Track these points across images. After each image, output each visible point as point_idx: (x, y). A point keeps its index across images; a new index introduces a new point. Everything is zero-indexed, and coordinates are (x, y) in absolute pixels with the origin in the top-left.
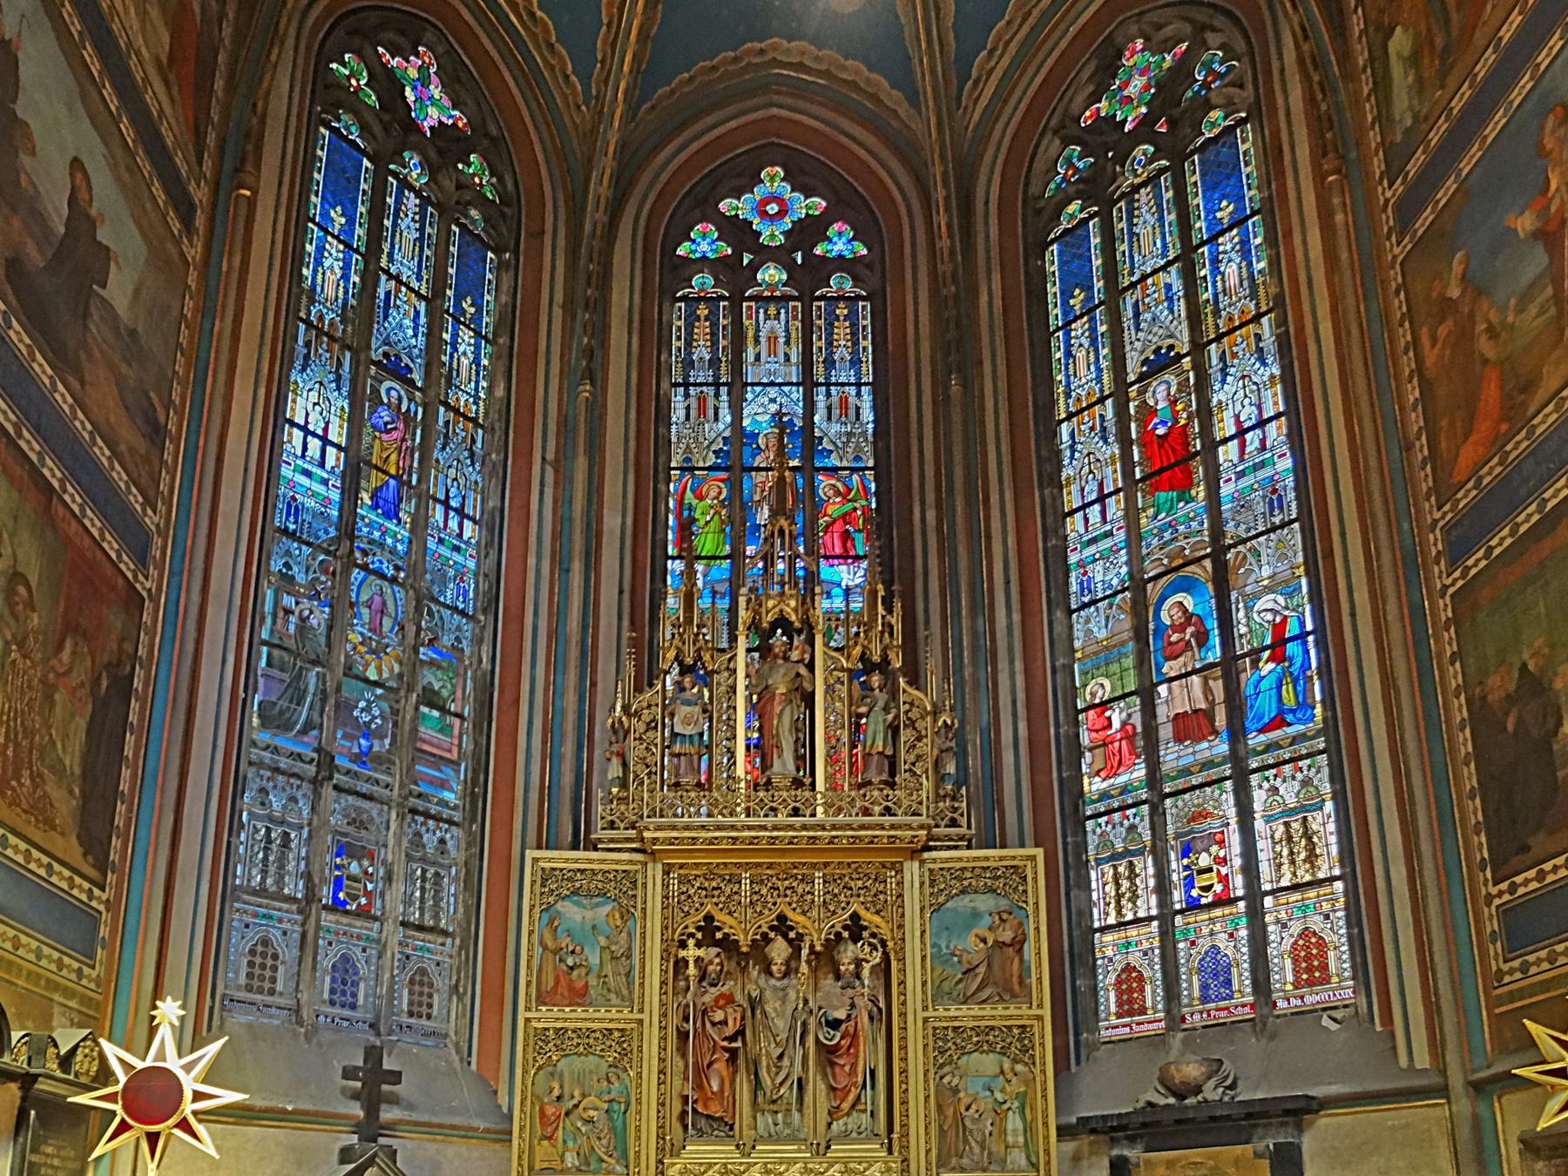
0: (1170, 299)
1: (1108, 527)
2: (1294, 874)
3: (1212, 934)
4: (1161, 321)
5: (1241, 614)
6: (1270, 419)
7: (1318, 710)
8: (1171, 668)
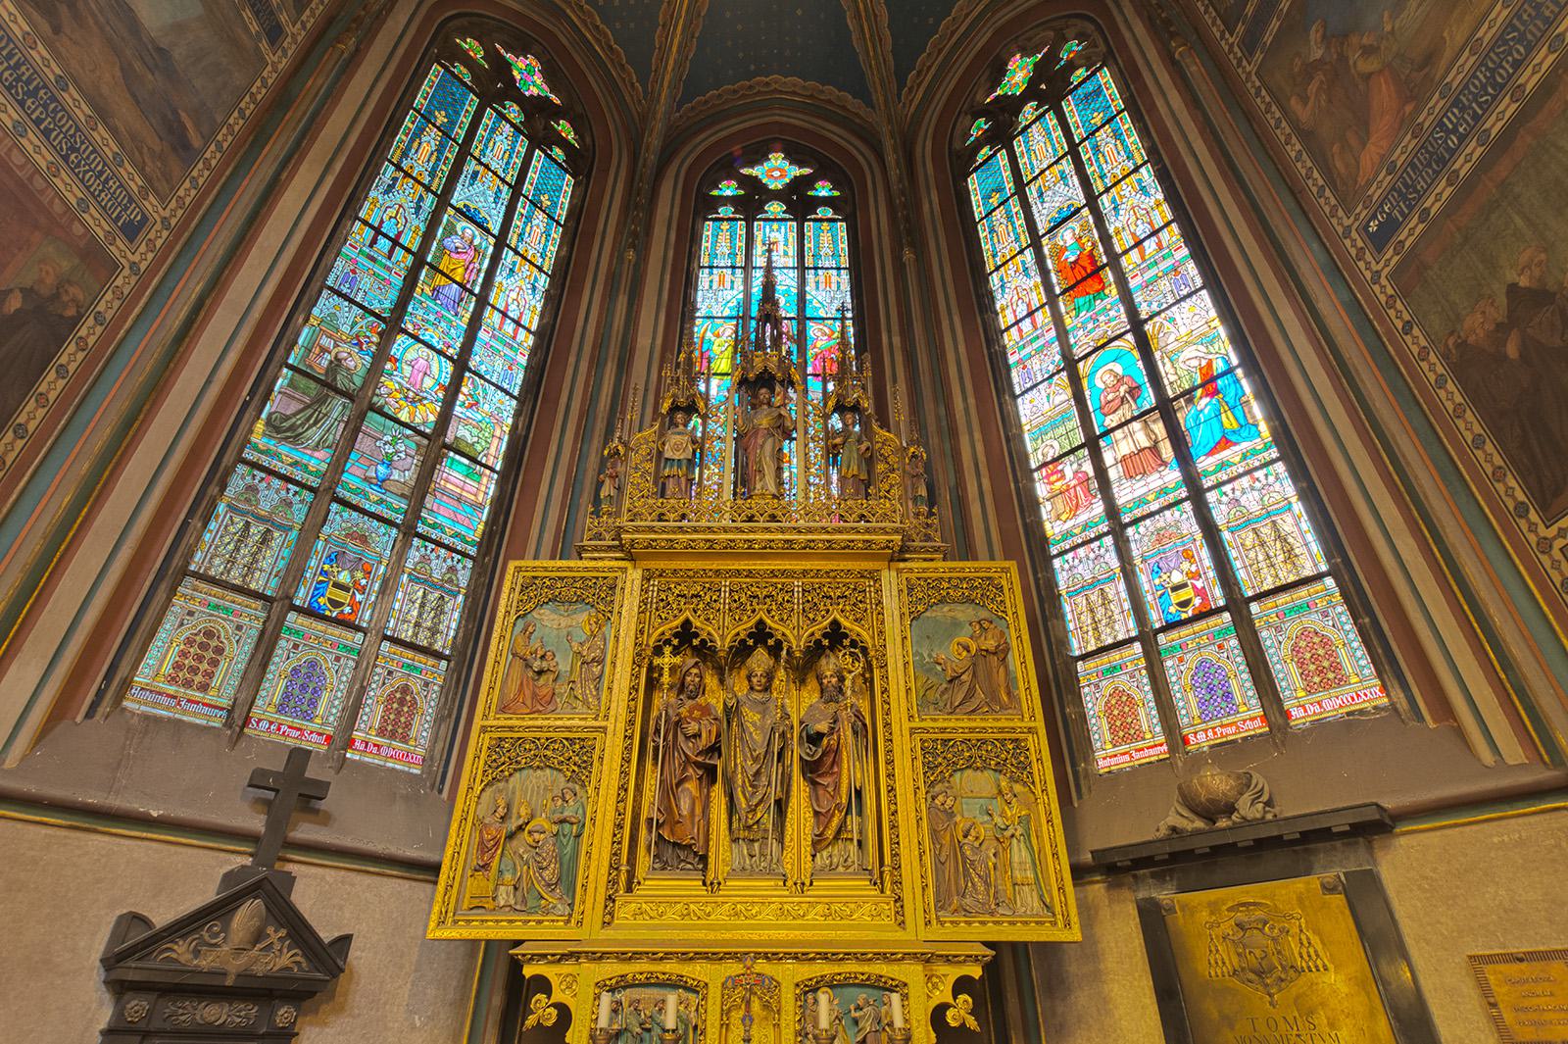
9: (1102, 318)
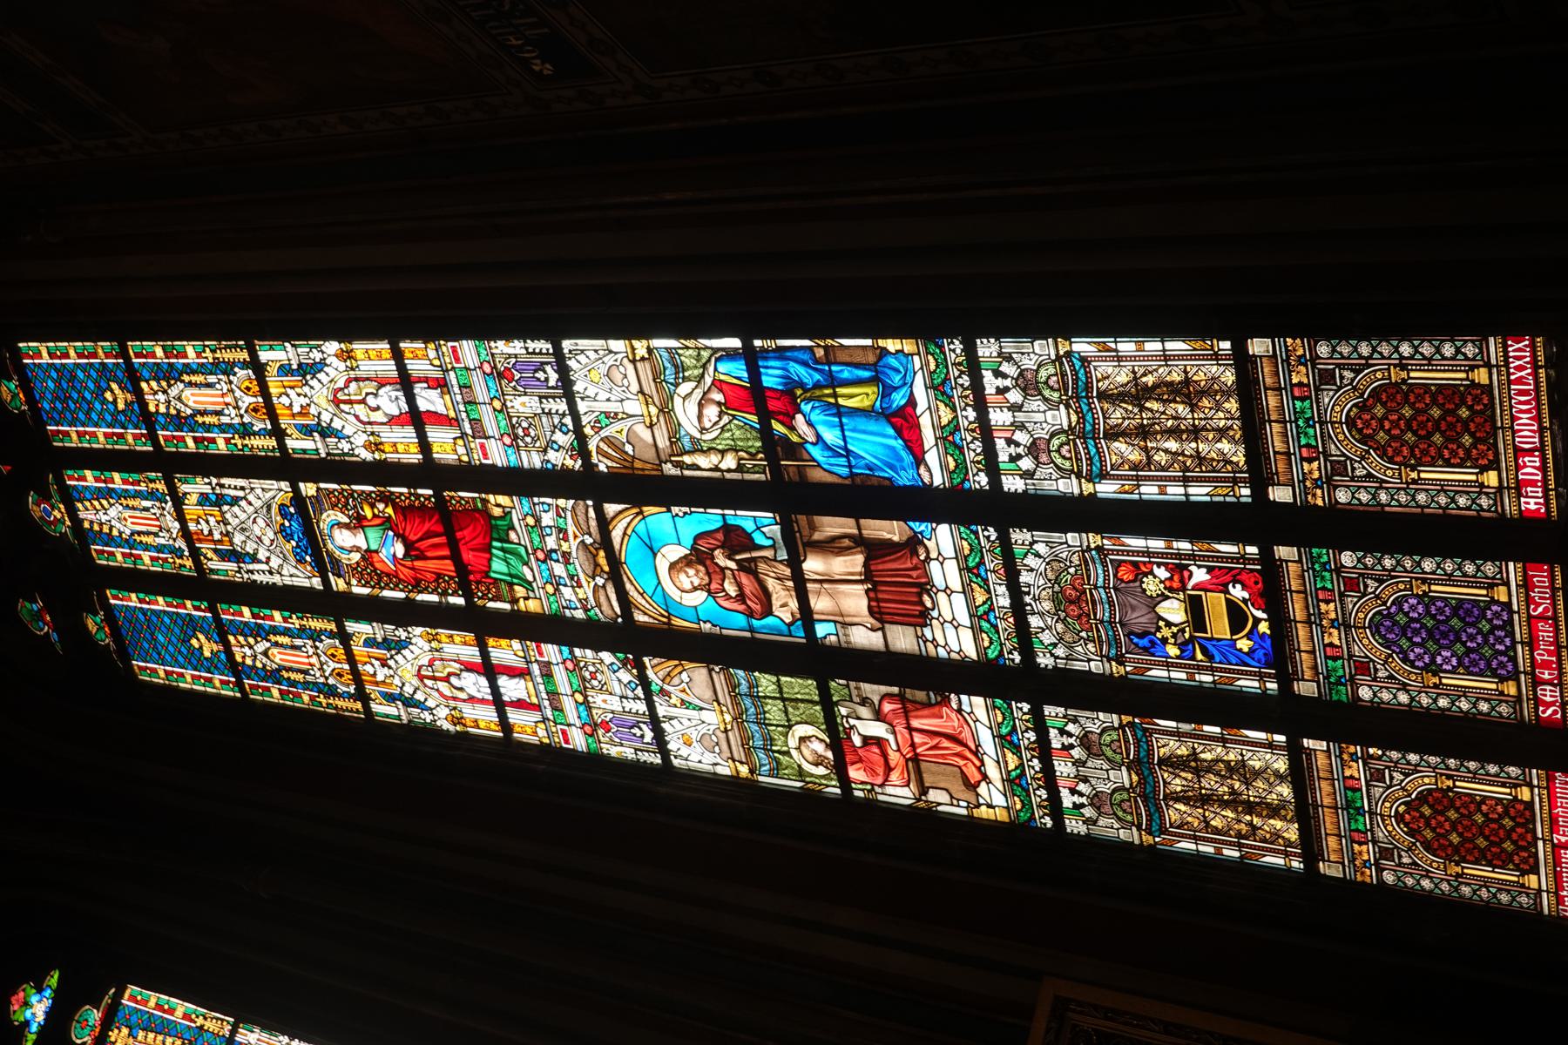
0: (220, 501)
1: (535, 669)
2: (1222, 433)
3: (1345, 625)
4: (251, 522)
5: (704, 461)
6: (401, 367)
7: (892, 345)
8: (785, 605)
9: (551, 542)
